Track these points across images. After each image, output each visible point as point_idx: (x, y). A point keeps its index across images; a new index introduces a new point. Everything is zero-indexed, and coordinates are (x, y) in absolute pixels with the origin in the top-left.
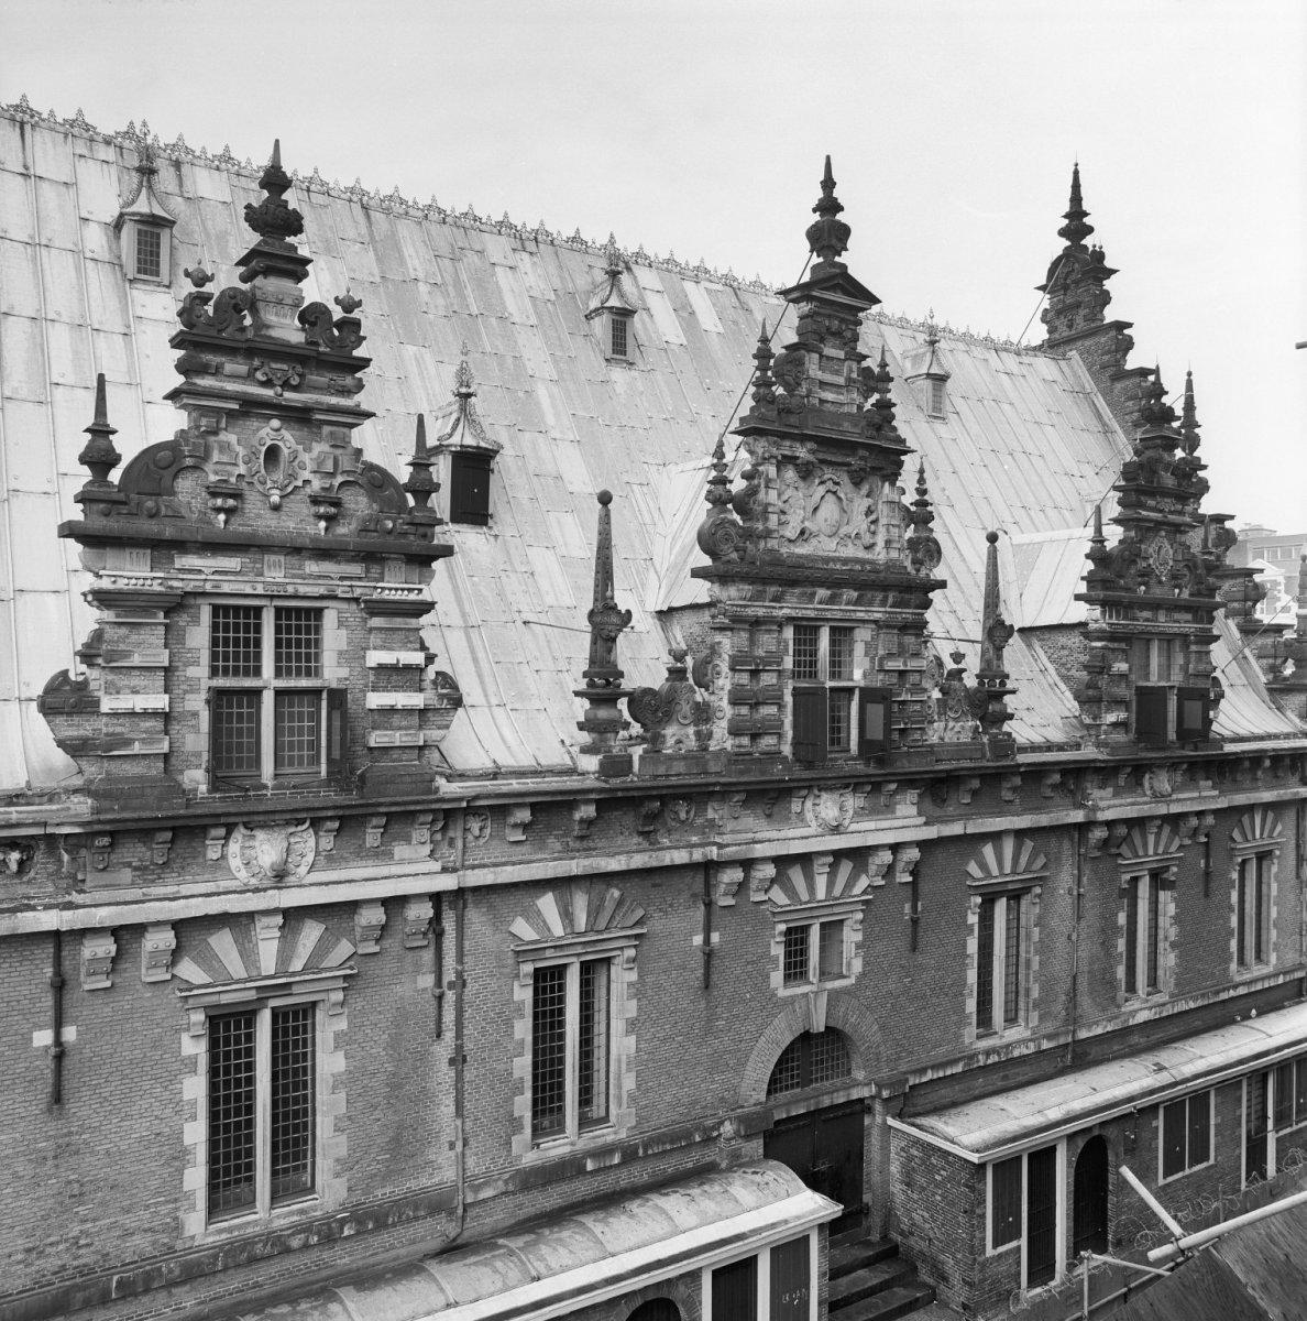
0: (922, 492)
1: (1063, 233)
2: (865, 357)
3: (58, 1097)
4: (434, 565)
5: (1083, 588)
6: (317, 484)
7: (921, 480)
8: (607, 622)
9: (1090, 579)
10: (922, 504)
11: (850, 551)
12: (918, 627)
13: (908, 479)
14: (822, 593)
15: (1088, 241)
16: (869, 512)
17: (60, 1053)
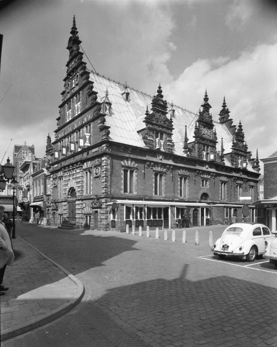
0: (215, 131)
1: (223, 106)
2: (210, 114)
3: (144, 178)
4: (172, 130)
5: (231, 147)
6: (164, 120)
7: (215, 130)
8: (186, 139)
9: (233, 146)
10: (215, 133)
11: (208, 137)
12: (215, 147)
13: (214, 129)
14: (206, 141)
15: (226, 108)
16: (210, 132)
17: (144, 173)
